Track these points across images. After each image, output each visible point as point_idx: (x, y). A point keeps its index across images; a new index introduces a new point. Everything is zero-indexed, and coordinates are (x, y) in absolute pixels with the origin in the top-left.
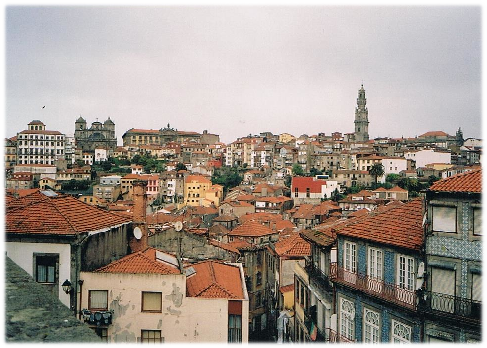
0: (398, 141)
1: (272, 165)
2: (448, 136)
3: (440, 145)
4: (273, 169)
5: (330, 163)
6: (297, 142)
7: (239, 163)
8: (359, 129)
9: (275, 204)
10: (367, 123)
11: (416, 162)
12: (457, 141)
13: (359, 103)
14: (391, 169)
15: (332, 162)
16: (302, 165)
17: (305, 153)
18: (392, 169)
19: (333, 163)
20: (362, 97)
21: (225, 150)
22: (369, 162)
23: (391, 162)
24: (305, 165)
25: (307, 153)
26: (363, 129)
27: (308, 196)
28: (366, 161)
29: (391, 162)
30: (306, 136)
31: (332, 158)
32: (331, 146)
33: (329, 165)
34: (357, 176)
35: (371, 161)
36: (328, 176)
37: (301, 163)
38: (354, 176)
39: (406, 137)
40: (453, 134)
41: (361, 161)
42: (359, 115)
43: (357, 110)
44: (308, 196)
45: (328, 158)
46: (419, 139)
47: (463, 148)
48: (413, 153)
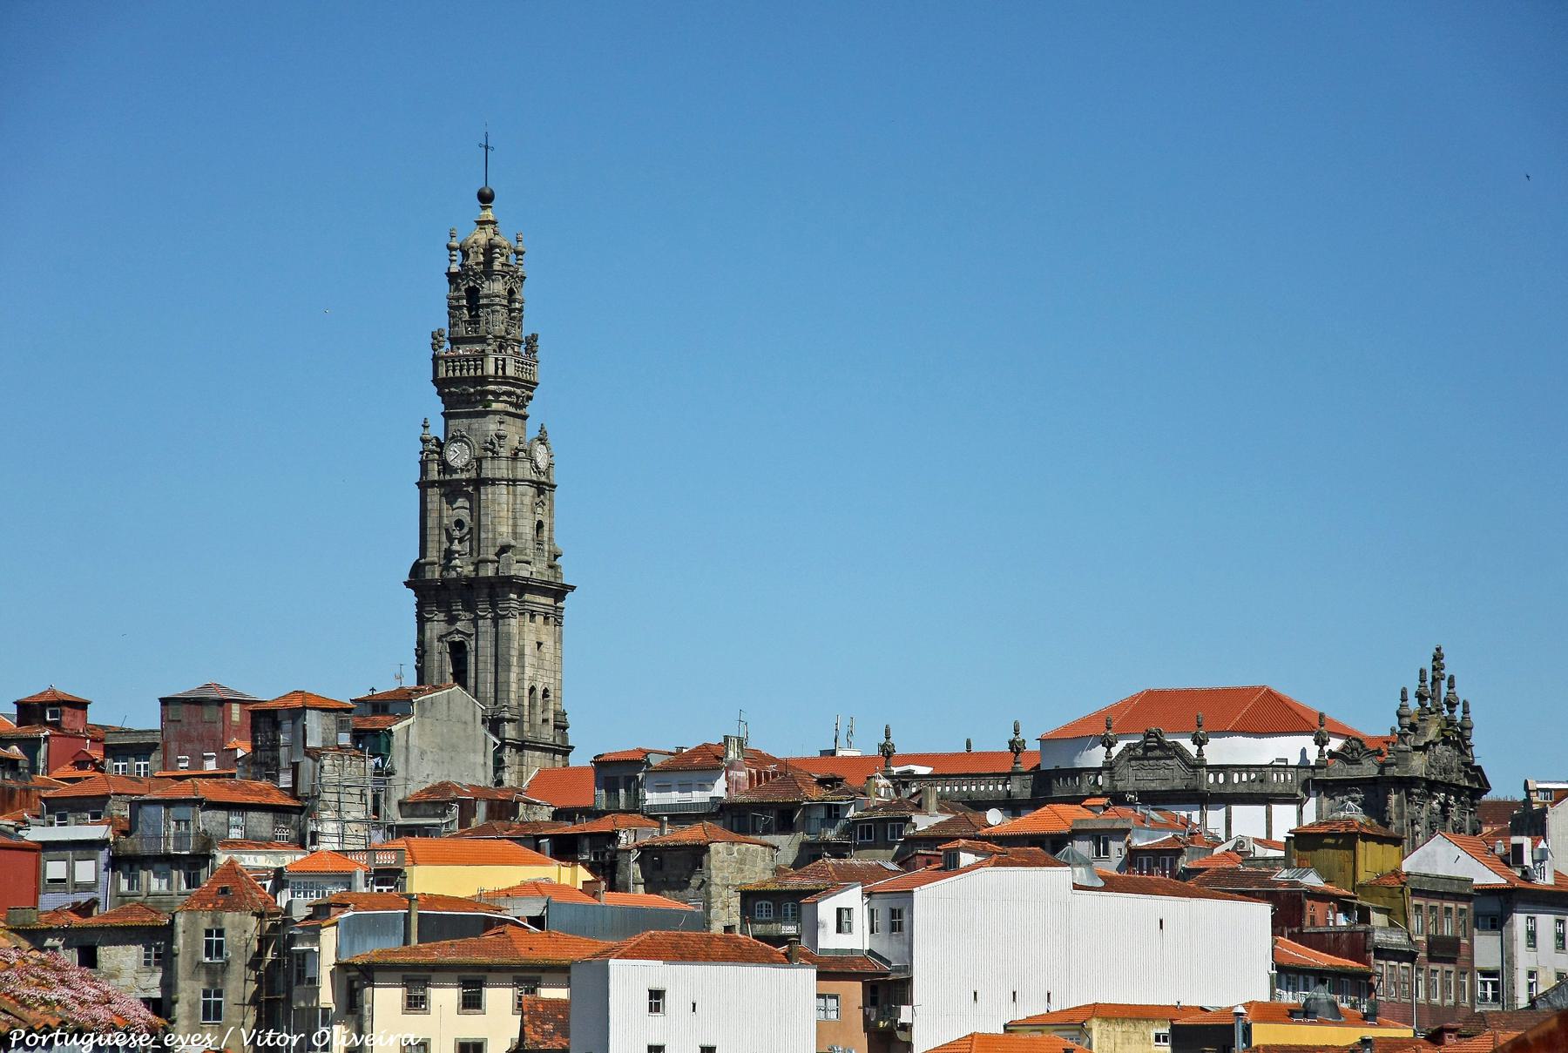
8: (458, 652)
22: (472, 1003)
23: (656, 996)
29: (656, 996)
31: (89, 959)
43: (434, 450)
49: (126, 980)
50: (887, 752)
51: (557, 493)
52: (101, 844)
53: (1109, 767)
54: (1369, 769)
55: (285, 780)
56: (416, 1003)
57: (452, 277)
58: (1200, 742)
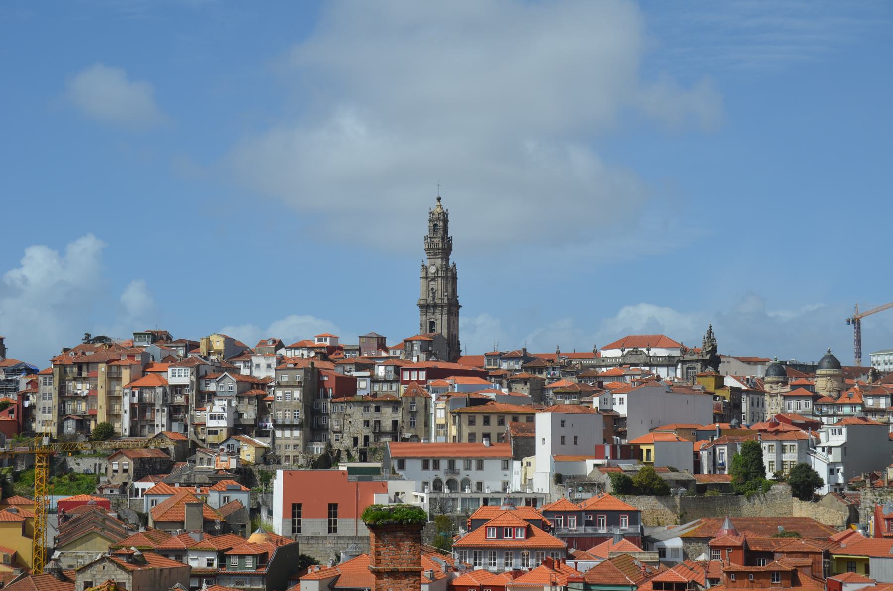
0: (549, 361)
1: (191, 430)
2: (684, 351)
3: (662, 372)
4: (194, 443)
5: (372, 423)
6: (255, 360)
7: (82, 423)
8: (432, 324)
9: (249, 563)
10: (453, 308)
11: (627, 422)
12: (705, 364)
13: (431, 251)
14: (563, 438)
15: (378, 423)
16: (287, 433)
17: (297, 394)
18: (566, 440)
19: (383, 425)
20: (440, 233)
21: (34, 384)
22: (487, 422)
23: (563, 422)
24: (296, 433)
25: (304, 394)
26: (445, 323)
27: (332, 529)
28: (479, 420)
29: (563, 422)
30: (279, 345)
31: (377, 409)
32: (367, 374)
33: (367, 431)
34: (460, 464)
35: (494, 420)
36: (378, 464)
37: (284, 427)
38: (452, 463)
39: (566, 349)
40: (695, 341)
41: (465, 419)
42: (433, 284)
43: (425, 268)
44: (332, 529)
45: (366, 408)
46: (605, 354)
47: (729, 382)
48: (617, 397)
49: (388, 415)
50: (558, 353)
51: (458, 281)
52: (368, 377)
53: (623, 357)
54: (695, 357)
55: (415, 359)
56: (472, 423)
57: (430, 221)
58: (649, 350)
